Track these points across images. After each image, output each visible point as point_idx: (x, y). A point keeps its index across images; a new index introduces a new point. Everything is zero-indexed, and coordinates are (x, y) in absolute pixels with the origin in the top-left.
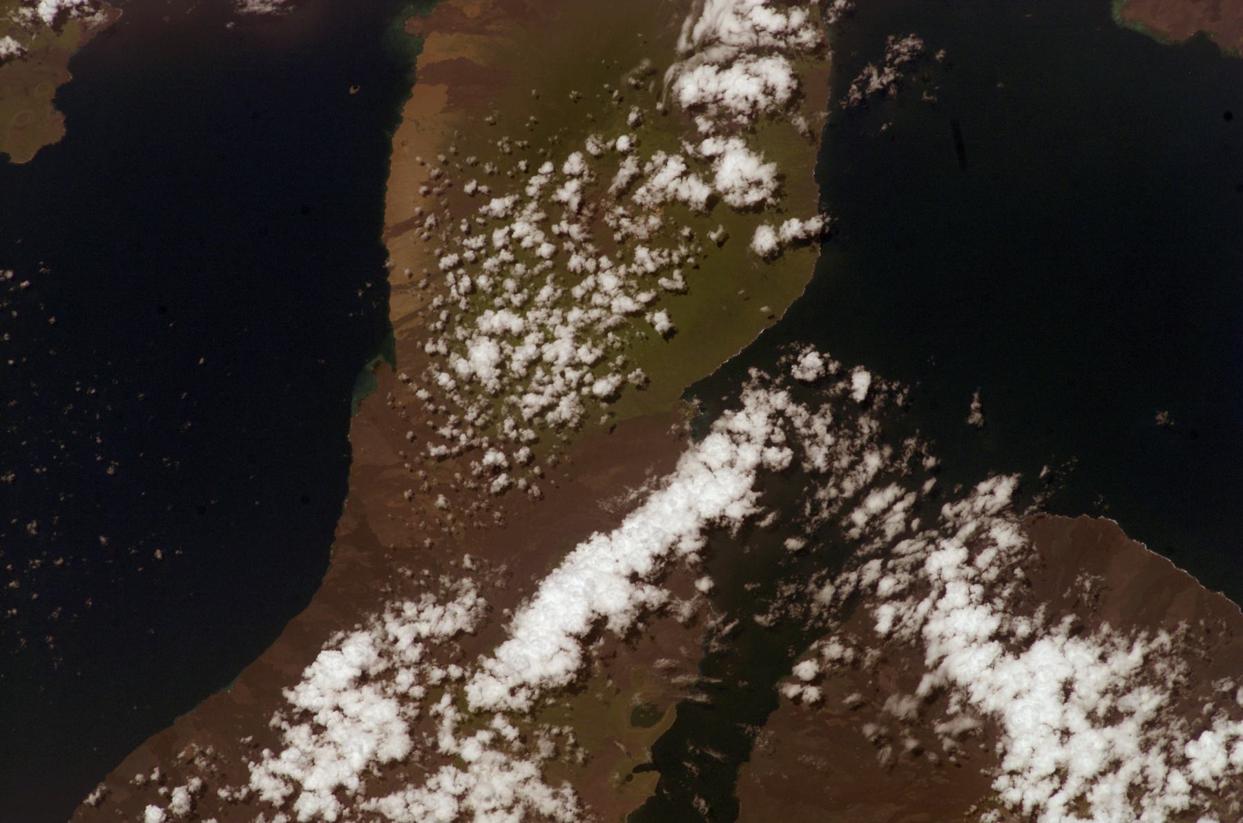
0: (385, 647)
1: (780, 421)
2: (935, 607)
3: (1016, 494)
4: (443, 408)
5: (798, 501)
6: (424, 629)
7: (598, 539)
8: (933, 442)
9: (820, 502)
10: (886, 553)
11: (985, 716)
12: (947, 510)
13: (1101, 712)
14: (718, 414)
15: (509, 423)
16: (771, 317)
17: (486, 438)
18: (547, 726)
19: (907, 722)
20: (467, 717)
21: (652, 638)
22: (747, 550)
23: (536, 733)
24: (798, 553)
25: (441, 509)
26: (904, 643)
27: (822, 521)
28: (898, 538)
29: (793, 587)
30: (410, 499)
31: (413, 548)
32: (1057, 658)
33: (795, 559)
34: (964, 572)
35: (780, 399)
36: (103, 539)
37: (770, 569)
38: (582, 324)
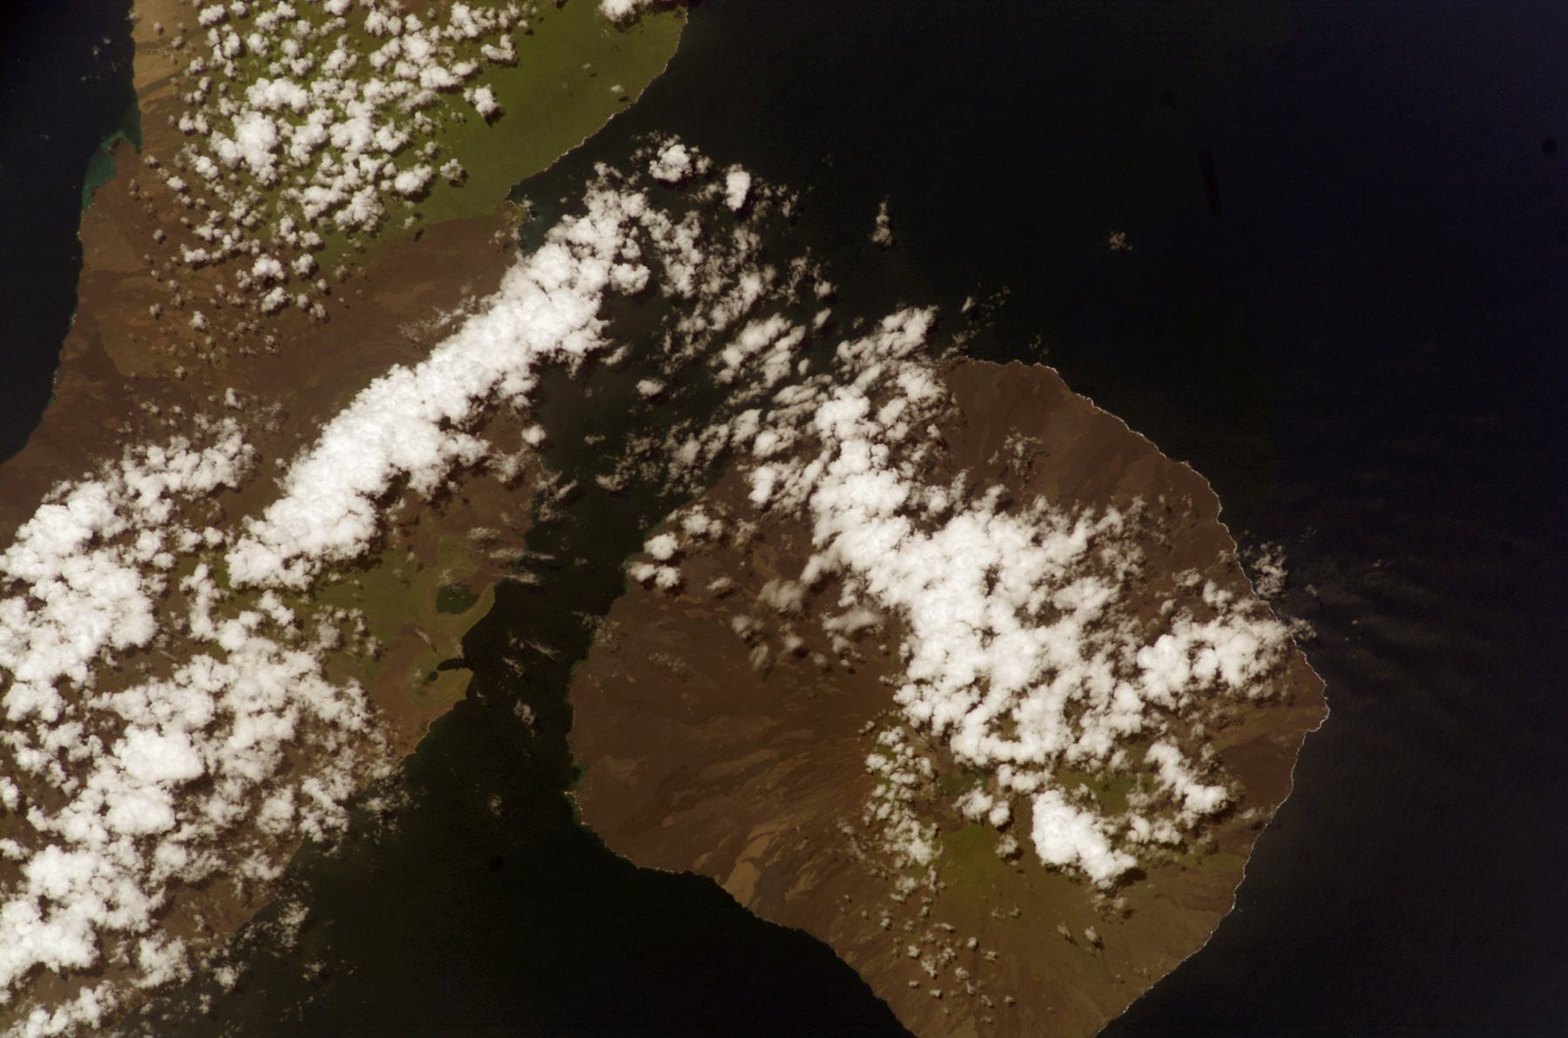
0: (123, 502)
1: (634, 231)
2: (826, 472)
3: (931, 332)
4: (202, 201)
5: (654, 334)
6: (174, 482)
7: (399, 373)
8: (828, 263)
9: (682, 335)
10: (766, 402)
11: (887, 609)
12: (844, 350)
13: (1033, 608)
14: (555, 220)
15: (286, 223)
16: (624, 99)
17: (257, 242)
18: (329, 608)
19: (787, 615)
20: (227, 593)
21: (466, 501)
22: (589, 393)
23: (316, 616)
24: (653, 399)
25: (198, 329)
26: (786, 516)
27: (685, 360)
28: (782, 383)
30: (157, 316)
31: (161, 379)
32: (981, 538)
33: (650, 407)
34: (863, 429)
35: (634, 204)
37: (618, 418)
38: (383, 101)
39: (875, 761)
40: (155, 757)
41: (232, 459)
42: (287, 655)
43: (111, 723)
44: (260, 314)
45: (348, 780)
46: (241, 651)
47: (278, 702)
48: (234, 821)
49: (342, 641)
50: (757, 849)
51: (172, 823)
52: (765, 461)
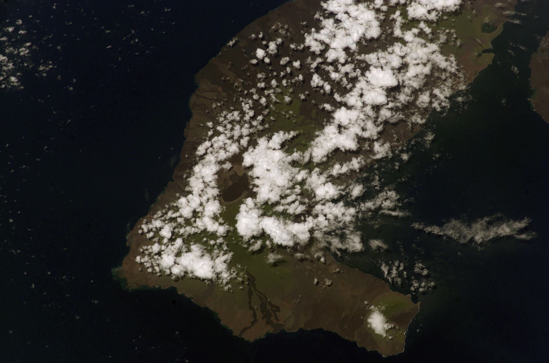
40: (380, 78)
43: (364, 65)
45: (450, 90)
46: (412, 42)
47: (425, 61)
48: (408, 102)
49: (448, 40)
51: (386, 102)
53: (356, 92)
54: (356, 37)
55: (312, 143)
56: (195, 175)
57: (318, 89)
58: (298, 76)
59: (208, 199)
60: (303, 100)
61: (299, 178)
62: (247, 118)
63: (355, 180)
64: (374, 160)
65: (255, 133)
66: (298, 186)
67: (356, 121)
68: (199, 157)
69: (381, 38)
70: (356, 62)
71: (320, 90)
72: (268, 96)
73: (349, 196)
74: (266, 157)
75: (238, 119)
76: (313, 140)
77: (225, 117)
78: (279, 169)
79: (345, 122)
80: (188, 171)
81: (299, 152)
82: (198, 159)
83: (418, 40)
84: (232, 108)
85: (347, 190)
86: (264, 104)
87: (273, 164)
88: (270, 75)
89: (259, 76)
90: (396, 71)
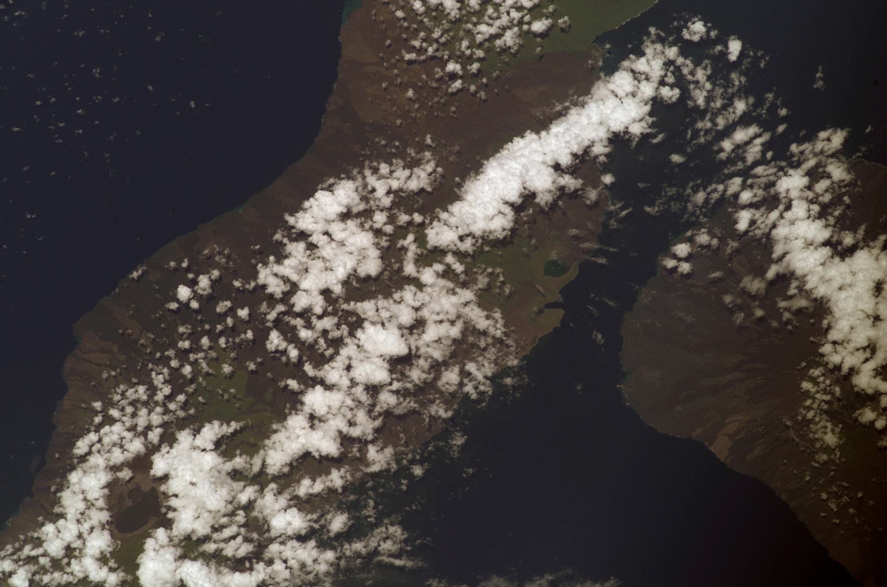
0: (364, 194)
1: (672, 68)
2: (782, 217)
5: (681, 128)
6: (395, 185)
7: (530, 136)
9: (698, 131)
10: (746, 173)
11: (815, 300)
12: (794, 148)
14: (625, 57)
18: (483, 266)
19: (754, 297)
20: (425, 252)
21: (564, 213)
23: (475, 270)
24: (679, 165)
25: (410, 99)
26: (757, 240)
27: (700, 146)
29: (674, 189)
30: (385, 89)
36: (150, 88)
37: (647, 176)
39: (806, 385)
40: (381, 340)
41: (430, 175)
42: (457, 290)
43: (354, 319)
44: (446, 93)
45: (493, 365)
46: (432, 286)
47: (452, 317)
48: (425, 382)
49: (489, 285)
50: (731, 429)
51: (389, 380)
52: (744, 207)
53: (340, 362)
54: (341, 273)
55: (267, 442)
56: (71, 487)
57: (277, 355)
58: (245, 333)
59: (92, 529)
60: (252, 371)
61: (244, 498)
62: (159, 397)
63: (335, 505)
64: (367, 474)
65: (172, 422)
66: (241, 513)
67: (339, 409)
68: (77, 458)
69: (382, 277)
70: (340, 313)
71: (282, 356)
72: (195, 364)
73: (325, 530)
74: (190, 462)
75: (145, 398)
76: (268, 438)
77: (123, 394)
78: (211, 483)
79: (321, 410)
80: (58, 480)
81: (244, 456)
82: (76, 461)
83: (442, 282)
84: (135, 380)
85: (323, 522)
86: (189, 376)
87: (201, 474)
88: (199, 329)
89: (182, 329)
90: (405, 331)
